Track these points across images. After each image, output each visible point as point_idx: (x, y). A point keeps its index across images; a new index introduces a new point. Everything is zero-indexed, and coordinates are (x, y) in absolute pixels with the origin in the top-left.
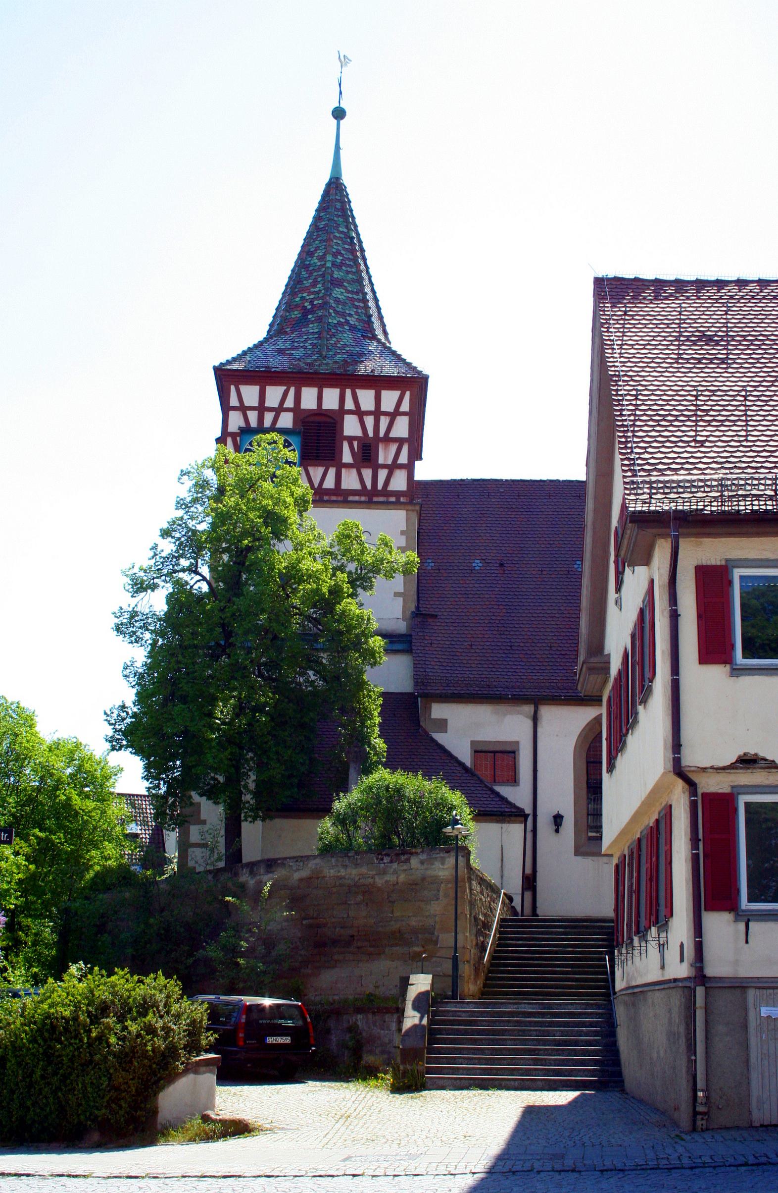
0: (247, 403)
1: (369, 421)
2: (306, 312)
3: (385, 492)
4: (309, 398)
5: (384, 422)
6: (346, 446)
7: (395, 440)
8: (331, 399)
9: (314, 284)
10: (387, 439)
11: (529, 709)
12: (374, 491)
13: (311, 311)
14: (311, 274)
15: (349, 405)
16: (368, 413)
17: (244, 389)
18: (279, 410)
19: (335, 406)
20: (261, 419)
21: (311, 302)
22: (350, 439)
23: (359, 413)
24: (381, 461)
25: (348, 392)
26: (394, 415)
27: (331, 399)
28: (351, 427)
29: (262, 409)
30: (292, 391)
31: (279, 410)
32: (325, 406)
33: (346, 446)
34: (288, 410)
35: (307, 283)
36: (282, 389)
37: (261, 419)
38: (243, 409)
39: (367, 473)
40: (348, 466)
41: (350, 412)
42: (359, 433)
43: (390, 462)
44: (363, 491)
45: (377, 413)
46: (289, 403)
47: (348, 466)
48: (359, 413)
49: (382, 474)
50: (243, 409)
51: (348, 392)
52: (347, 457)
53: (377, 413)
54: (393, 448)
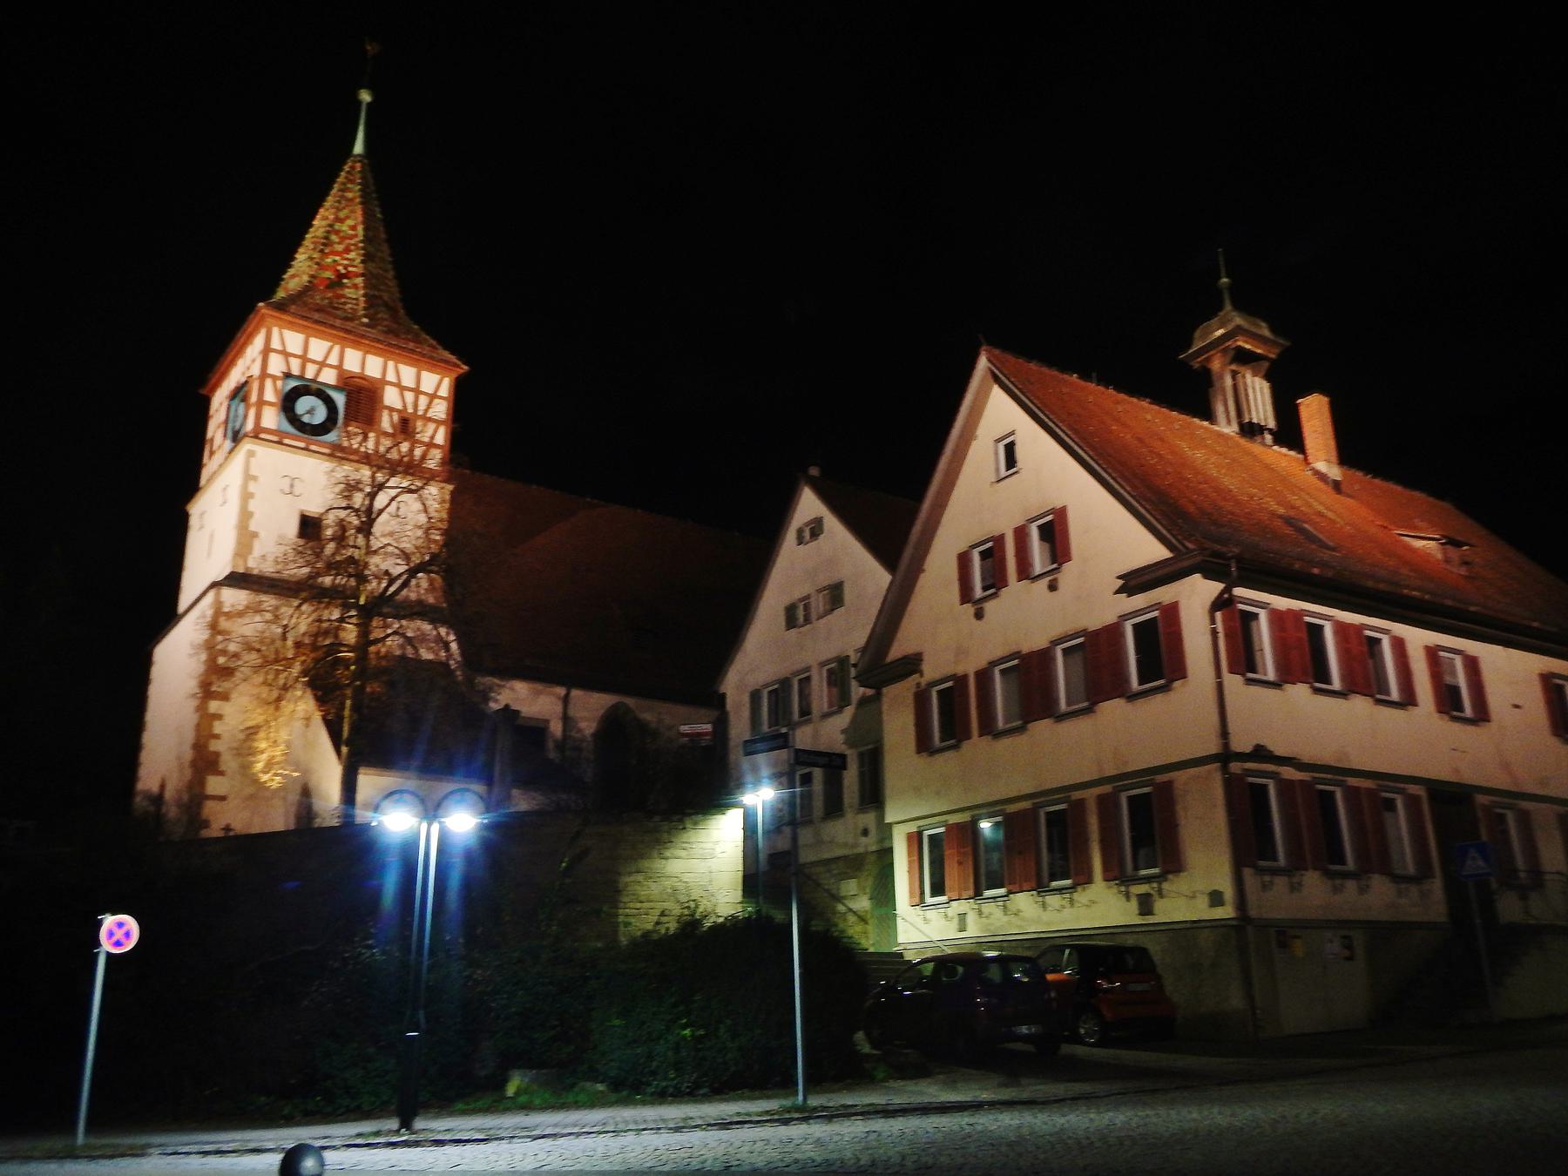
0: (290, 349)
1: (409, 396)
2: (341, 276)
4: (353, 360)
5: (423, 401)
7: (430, 419)
8: (374, 366)
9: (347, 250)
11: (561, 691)
13: (346, 276)
14: (343, 239)
17: (288, 334)
18: (322, 364)
19: (378, 376)
20: (303, 368)
21: (346, 267)
22: (392, 410)
23: (402, 389)
27: (374, 366)
28: (391, 397)
29: (304, 359)
30: (337, 349)
31: (322, 364)
33: (385, 414)
34: (331, 366)
35: (340, 248)
36: (326, 344)
37: (303, 368)
38: (286, 354)
40: (386, 434)
42: (399, 406)
46: (333, 360)
50: (286, 354)
53: (417, 391)
54: (432, 426)
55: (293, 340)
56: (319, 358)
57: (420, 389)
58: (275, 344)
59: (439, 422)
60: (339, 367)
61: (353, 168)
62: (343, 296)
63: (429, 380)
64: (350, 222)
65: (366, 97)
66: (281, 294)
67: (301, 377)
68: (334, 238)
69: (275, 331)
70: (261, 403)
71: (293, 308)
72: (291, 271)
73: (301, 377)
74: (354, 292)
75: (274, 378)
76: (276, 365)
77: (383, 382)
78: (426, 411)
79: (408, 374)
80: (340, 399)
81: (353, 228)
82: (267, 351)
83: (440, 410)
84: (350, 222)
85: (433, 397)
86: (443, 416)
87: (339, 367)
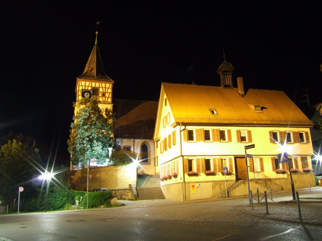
0: (83, 85)
1: (104, 89)
2: (92, 69)
3: (107, 102)
5: (107, 89)
6: (100, 93)
8: (97, 85)
9: (93, 63)
10: (107, 92)
11: (133, 140)
12: (105, 101)
13: (93, 68)
14: (93, 61)
15: (101, 86)
16: (104, 88)
17: (82, 82)
18: (88, 86)
22: (101, 92)
23: (102, 88)
24: (106, 96)
25: (100, 84)
26: (109, 88)
27: (97, 85)
28: (101, 90)
29: (85, 86)
31: (88, 86)
32: (96, 86)
33: (100, 93)
35: (92, 63)
38: (82, 86)
39: (104, 98)
41: (101, 87)
42: (102, 91)
43: (108, 96)
44: (103, 101)
45: (105, 88)
46: (90, 85)
47: (101, 97)
48: (102, 88)
49: (106, 98)
50: (82, 86)
51: (100, 84)
52: (100, 95)
53: (105, 88)
55: (83, 83)
56: (88, 85)
57: (106, 88)
58: (80, 84)
59: (110, 93)
60: (91, 86)
61: (95, 47)
62: (93, 72)
63: (108, 85)
64: (94, 58)
65: (97, 33)
66: (84, 73)
67: (85, 89)
68: (91, 61)
69: (80, 82)
70: (79, 95)
71: (82, 77)
72: (85, 69)
73: (85, 89)
74: (94, 72)
75: (80, 90)
76: (81, 88)
77: (99, 87)
78: (107, 91)
79: (104, 85)
80: (92, 92)
81: (95, 59)
82: (79, 86)
83: (110, 91)
84: (94, 58)
85: (109, 88)
86: (110, 92)
87: (91, 86)
